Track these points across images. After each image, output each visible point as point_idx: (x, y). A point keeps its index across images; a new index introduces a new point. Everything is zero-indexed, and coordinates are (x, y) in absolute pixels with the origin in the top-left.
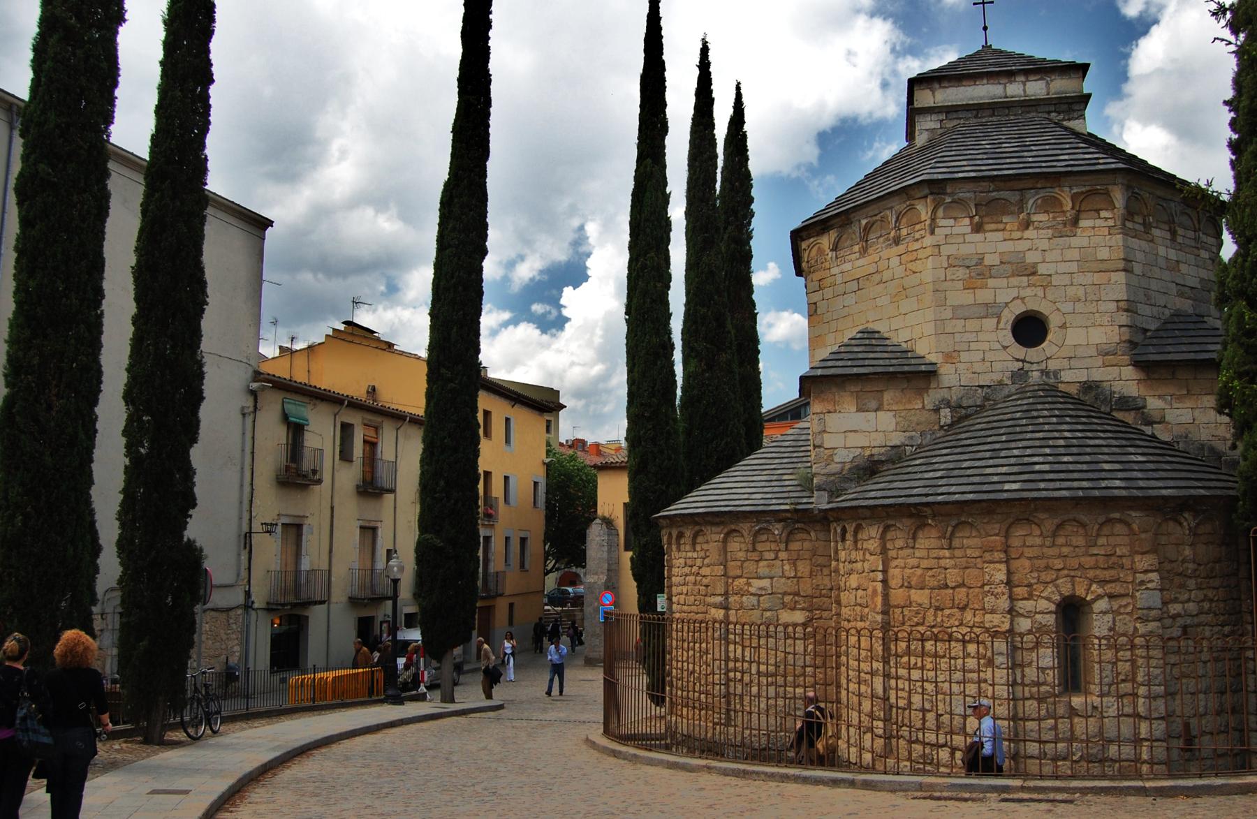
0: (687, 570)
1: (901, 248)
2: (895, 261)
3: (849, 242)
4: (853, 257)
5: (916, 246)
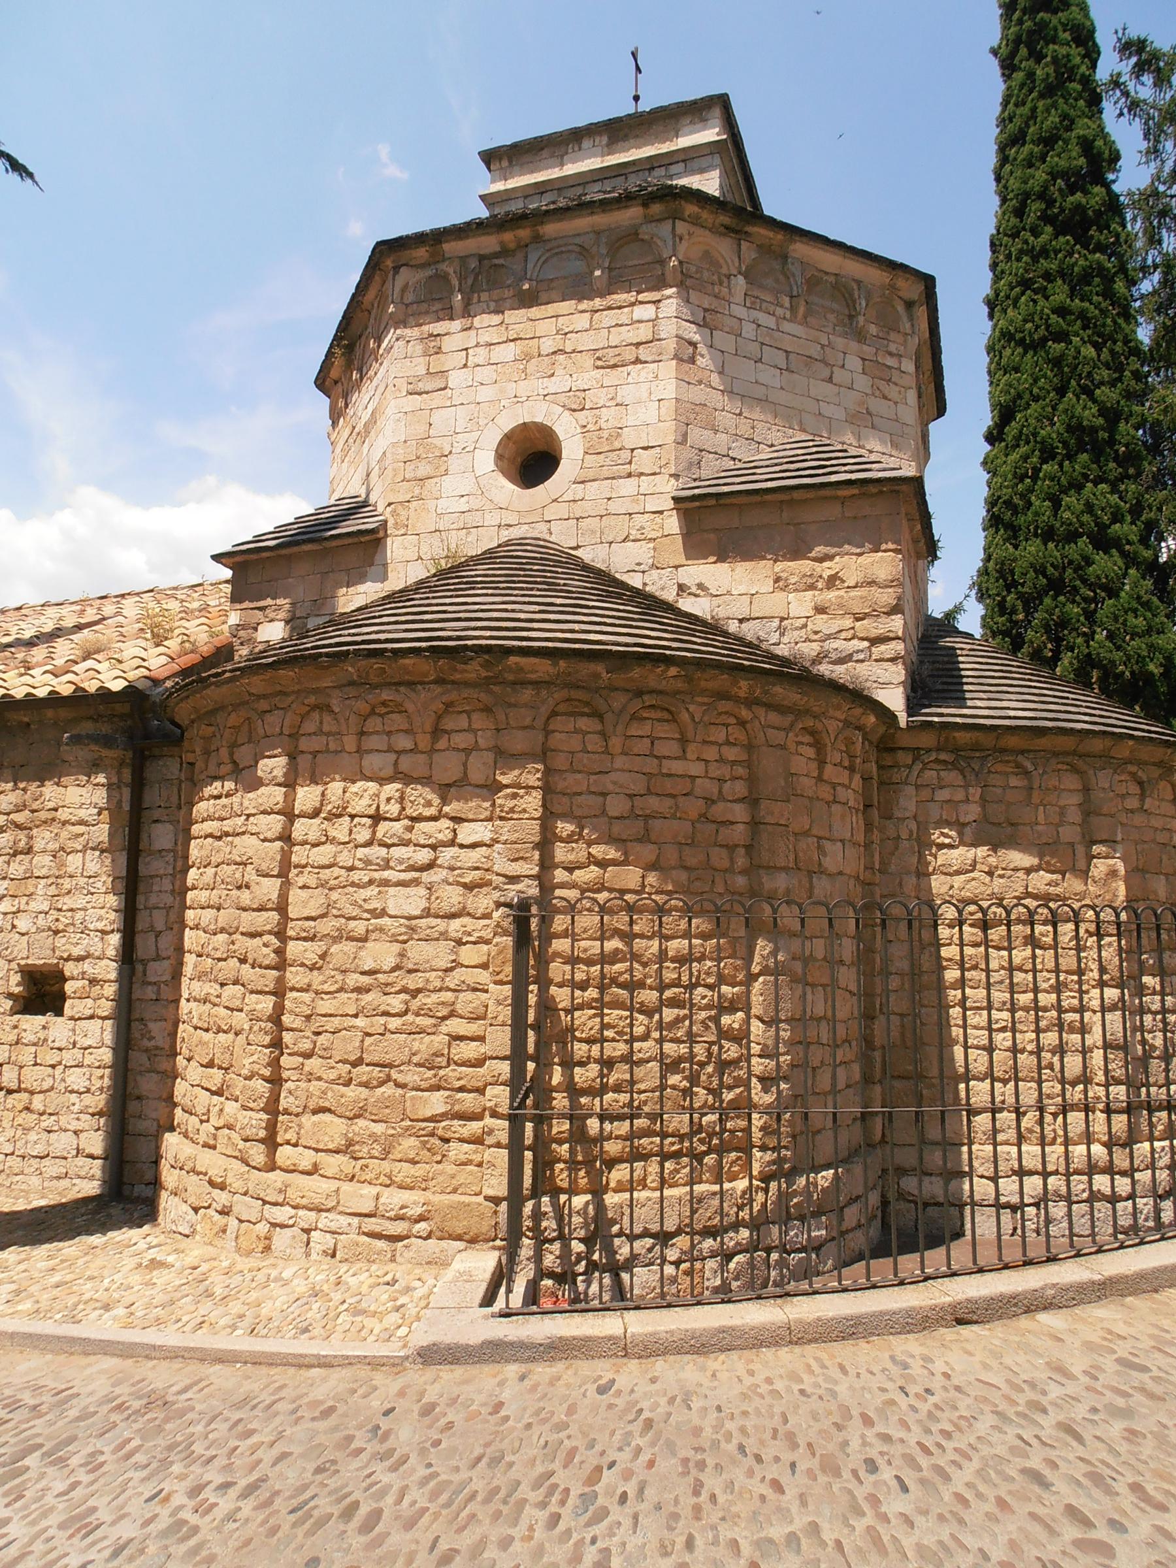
0: (654, 803)
1: (868, 351)
2: (854, 363)
3: (769, 282)
4: (779, 311)
5: (891, 362)
